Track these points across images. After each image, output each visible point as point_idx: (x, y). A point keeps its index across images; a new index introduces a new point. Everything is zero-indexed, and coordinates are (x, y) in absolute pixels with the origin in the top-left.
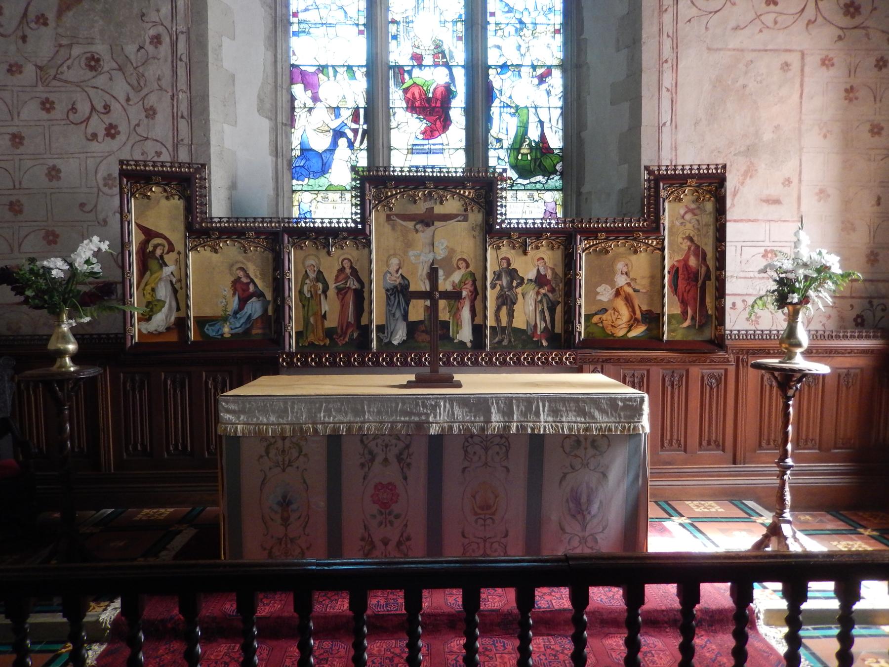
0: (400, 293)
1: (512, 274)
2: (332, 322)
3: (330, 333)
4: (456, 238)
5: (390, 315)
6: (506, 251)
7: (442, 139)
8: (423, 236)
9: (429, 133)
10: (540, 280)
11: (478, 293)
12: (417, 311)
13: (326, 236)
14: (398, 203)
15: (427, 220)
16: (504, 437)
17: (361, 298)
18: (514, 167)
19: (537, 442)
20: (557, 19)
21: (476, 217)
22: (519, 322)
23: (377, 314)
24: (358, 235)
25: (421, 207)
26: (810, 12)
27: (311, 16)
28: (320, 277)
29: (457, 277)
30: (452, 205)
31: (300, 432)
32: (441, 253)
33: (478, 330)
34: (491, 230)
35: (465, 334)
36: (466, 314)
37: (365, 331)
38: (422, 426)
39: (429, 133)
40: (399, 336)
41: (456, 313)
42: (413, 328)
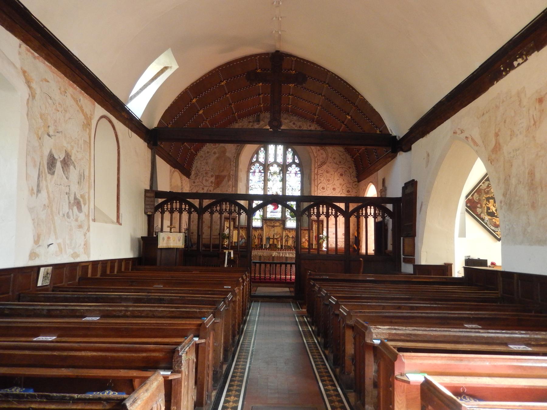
0: (268, 239)
1: (288, 236)
2: (256, 244)
3: (256, 245)
4: (278, 230)
5: (266, 242)
6: (287, 232)
7: (277, 210)
8: (273, 229)
9: (275, 209)
10: (293, 237)
11: (282, 239)
12: (271, 242)
13: (256, 229)
14: (268, 223)
15: (273, 226)
16: (282, 257)
17: (261, 240)
18: (291, 216)
19: (287, 257)
20: (300, 188)
21: (282, 226)
22: (289, 245)
23: (264, 243)
24: (261, 228)
25: (273, 224)
26: (341, 192)
27: (253, 187)
28: (255, 236)
29: (278, 236)
30: (278, 224)
31: (256, 255)
32: (276, 232)
33: (282, 246)
34: (284, 229)
35: (279, 246)
36: (280, 243)
37: (262, 245)
38: (272, 255)
39: (275, 209)
40: (268, 246)
41: (278, 242)
42: (270, 245)
